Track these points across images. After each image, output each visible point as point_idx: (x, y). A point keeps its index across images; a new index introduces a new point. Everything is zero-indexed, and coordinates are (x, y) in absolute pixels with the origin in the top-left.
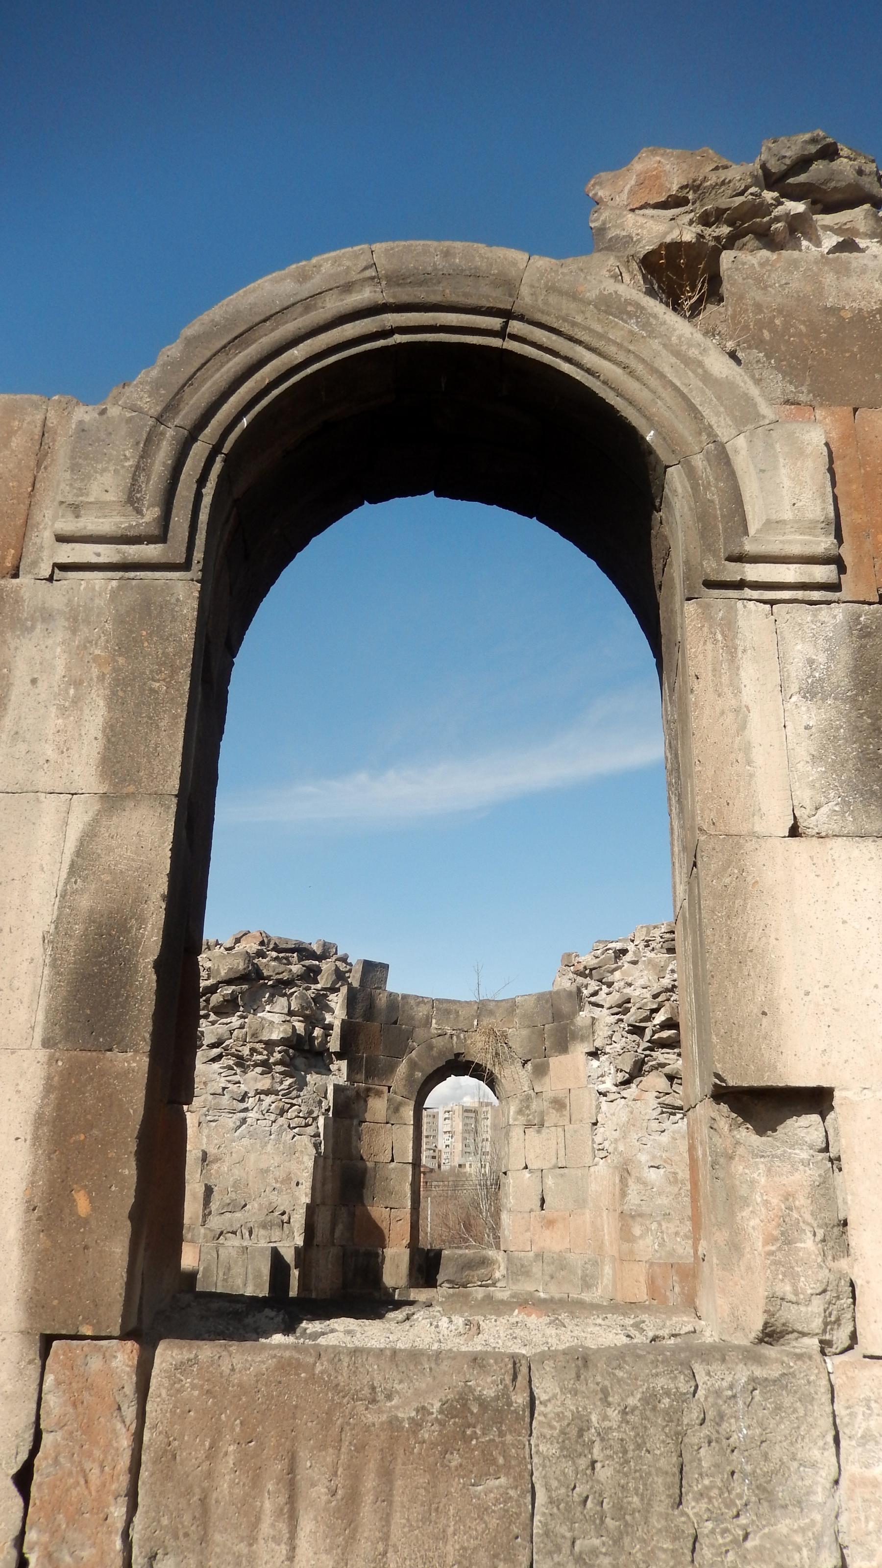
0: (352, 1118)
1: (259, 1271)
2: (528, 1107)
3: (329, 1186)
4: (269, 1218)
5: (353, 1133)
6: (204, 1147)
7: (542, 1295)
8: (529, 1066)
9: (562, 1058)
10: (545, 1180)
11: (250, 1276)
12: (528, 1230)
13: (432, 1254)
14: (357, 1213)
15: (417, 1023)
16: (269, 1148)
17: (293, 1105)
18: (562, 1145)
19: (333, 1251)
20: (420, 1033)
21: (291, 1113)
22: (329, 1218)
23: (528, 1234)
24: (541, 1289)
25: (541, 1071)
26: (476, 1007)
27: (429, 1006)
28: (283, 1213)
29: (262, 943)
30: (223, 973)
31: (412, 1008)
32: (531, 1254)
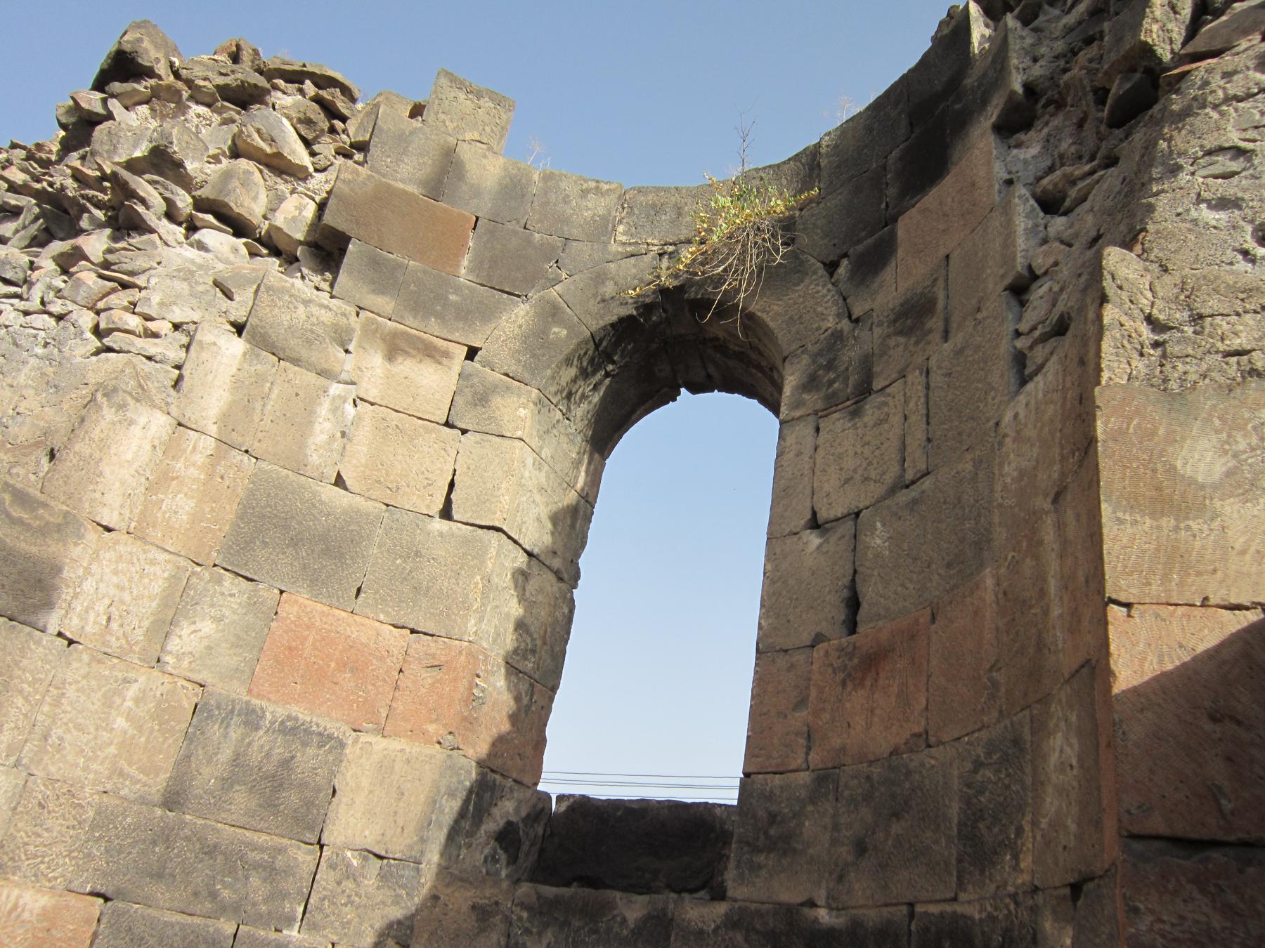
2: (830, 366)
3: (180, 506)
5: (324, 410)
7: (824, 916)
8: (843, 270)
9: (931, 199)
10: (865, 539)
12: (801, 703)
14: (289, 610)
15: (575, 232)
18: (917, 419)
20: (582, 250)
22: (157, 587)
23: (803, 714)
24: (821, 896)
25: (874, 262)
27: (611, 200)
31: (566, 200)
32: (804, 777)
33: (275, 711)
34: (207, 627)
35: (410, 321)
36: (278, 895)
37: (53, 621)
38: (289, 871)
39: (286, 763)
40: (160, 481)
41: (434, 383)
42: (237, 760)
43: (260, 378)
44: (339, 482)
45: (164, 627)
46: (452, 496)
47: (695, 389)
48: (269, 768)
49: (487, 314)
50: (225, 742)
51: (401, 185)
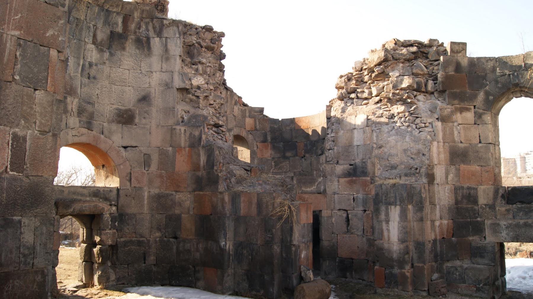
0: (453, 122)
1: (402, 194)
3: (442, 156)
4: (409, 171)
5: (455, 130)
6: (375, 141)
11: (398, 198)
13: (510, 189)
14: (461, 168)
16: (407, 139)
17: (417, 117)
19: (448, 187)
20: (490, 76)
21: (418, 121)
22: (444, 171)
26: (522, 57)
28: (417, 169)
29: (396, 44)
30: (376, 59)
31: (483, 64)
33: (465, 186)
34: (452, 175)
35: (462, 104)
36: (475, 214)
37: (435, 182)
38: (475, 210)
39: (469, 194)
40: (439, 153)
41: (470, 116)
42: (462, 194)
43: (445, 128)
44: (461, 142)
45: (447, 178)
46: (481, 138)
47: (516, 97)
48: (468, 195)
49: (475, 97)
50: (460, 193)
51: (450, 73)
